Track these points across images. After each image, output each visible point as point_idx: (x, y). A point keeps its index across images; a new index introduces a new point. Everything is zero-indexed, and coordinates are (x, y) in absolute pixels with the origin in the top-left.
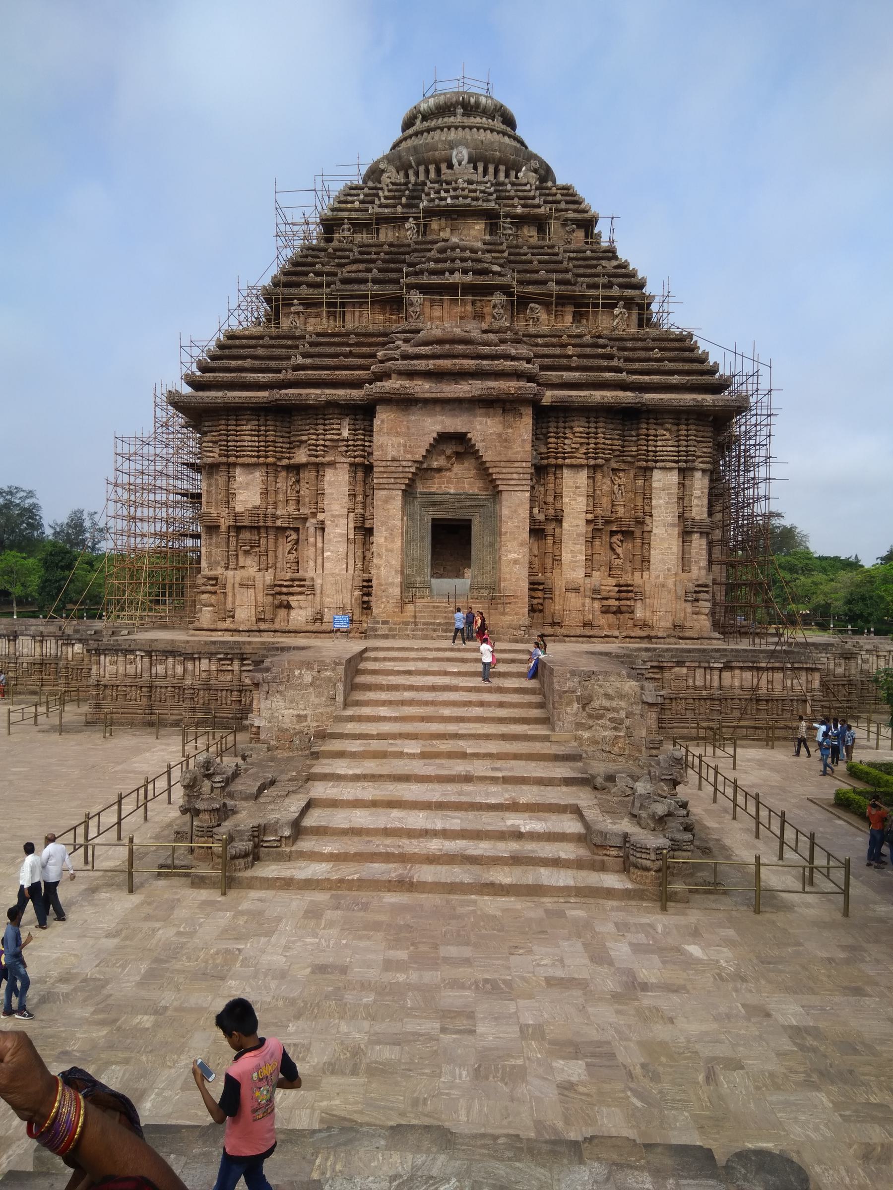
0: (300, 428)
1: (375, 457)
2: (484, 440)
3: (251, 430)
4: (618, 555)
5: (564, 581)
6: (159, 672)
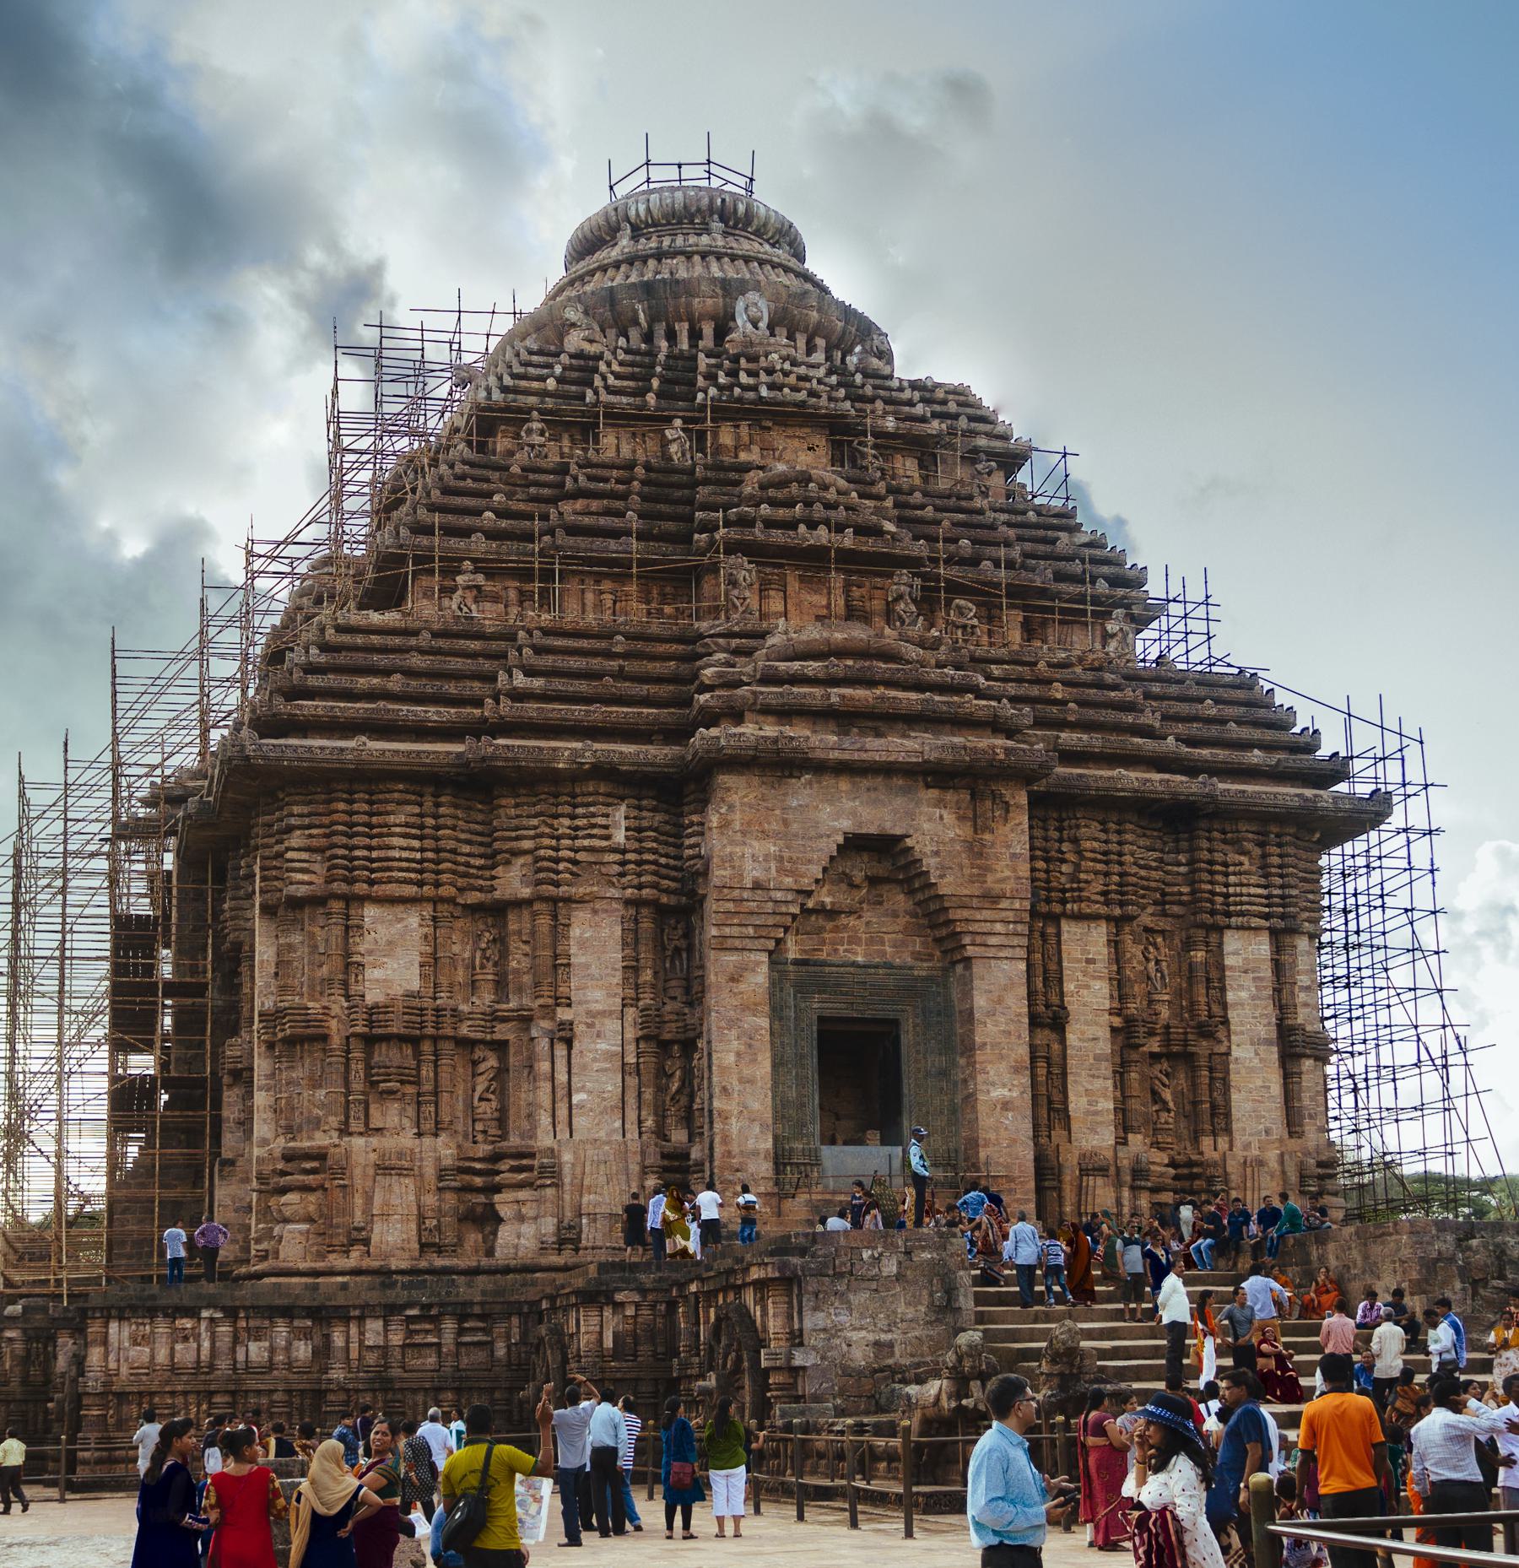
0: (515, 822)
1: (716, 881)
2: (937, 853)
3: (407, 825)
4: (1165, 1103)
6: (253, 1356)
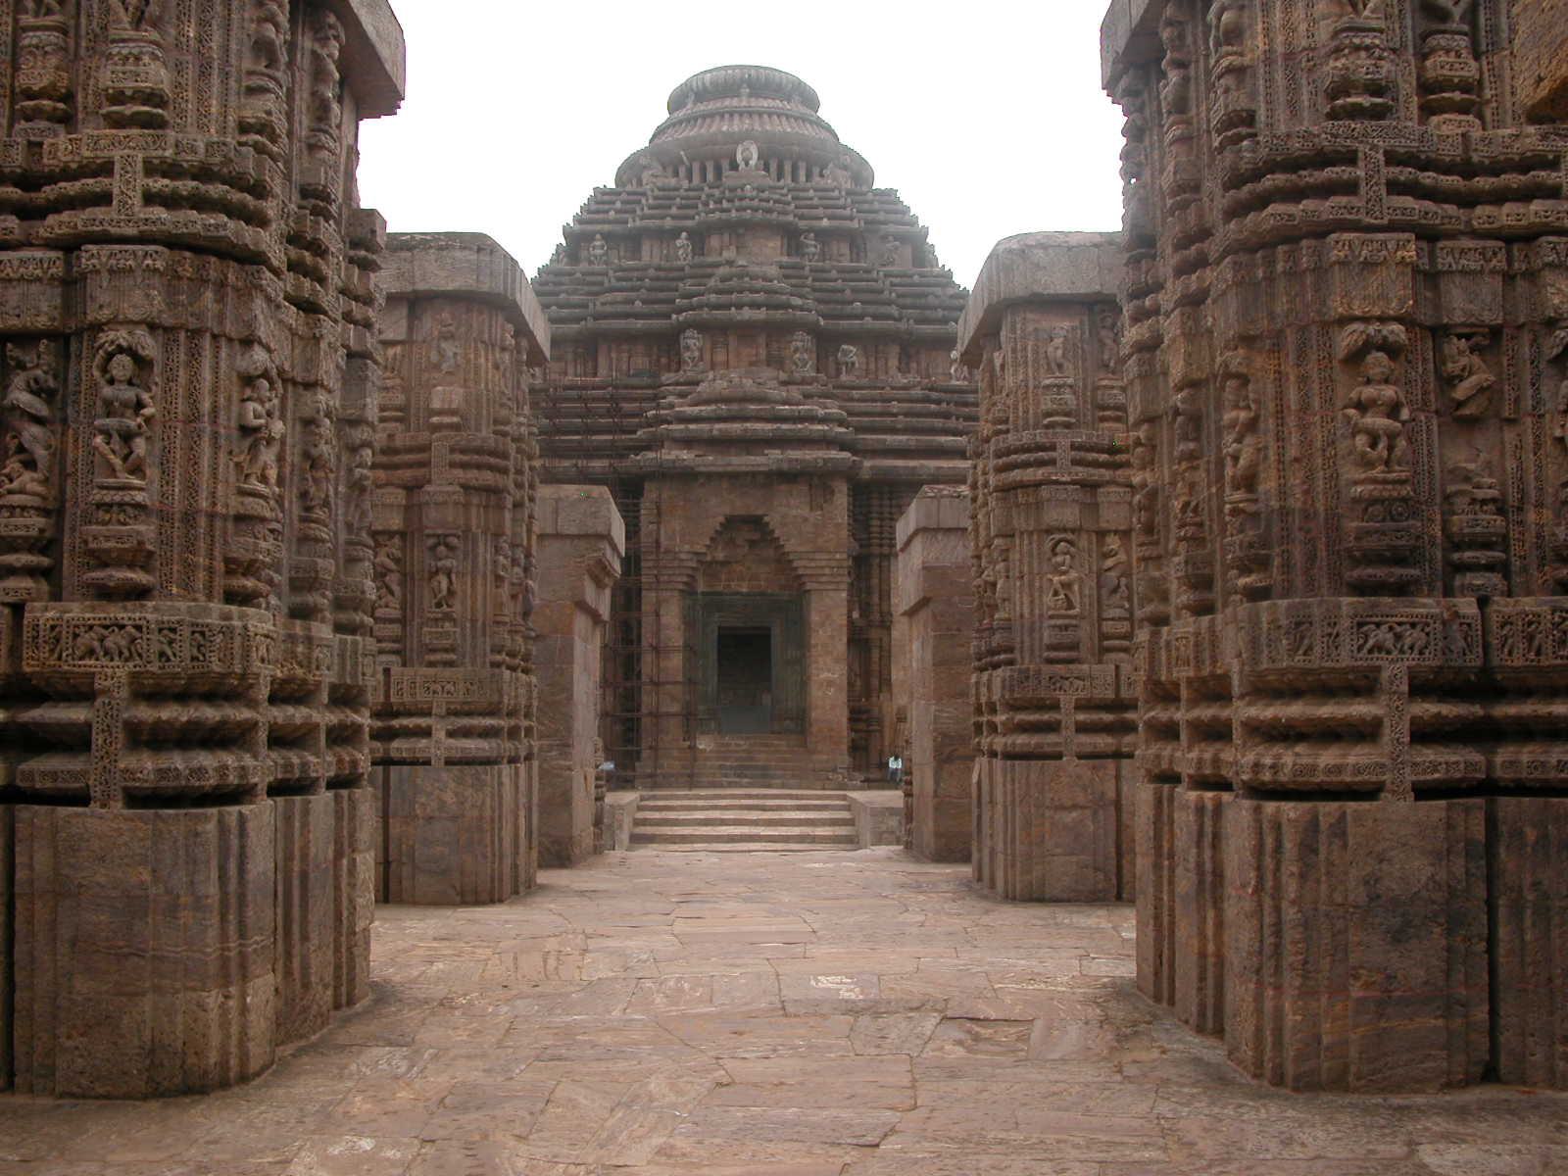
5: (895, 707)
